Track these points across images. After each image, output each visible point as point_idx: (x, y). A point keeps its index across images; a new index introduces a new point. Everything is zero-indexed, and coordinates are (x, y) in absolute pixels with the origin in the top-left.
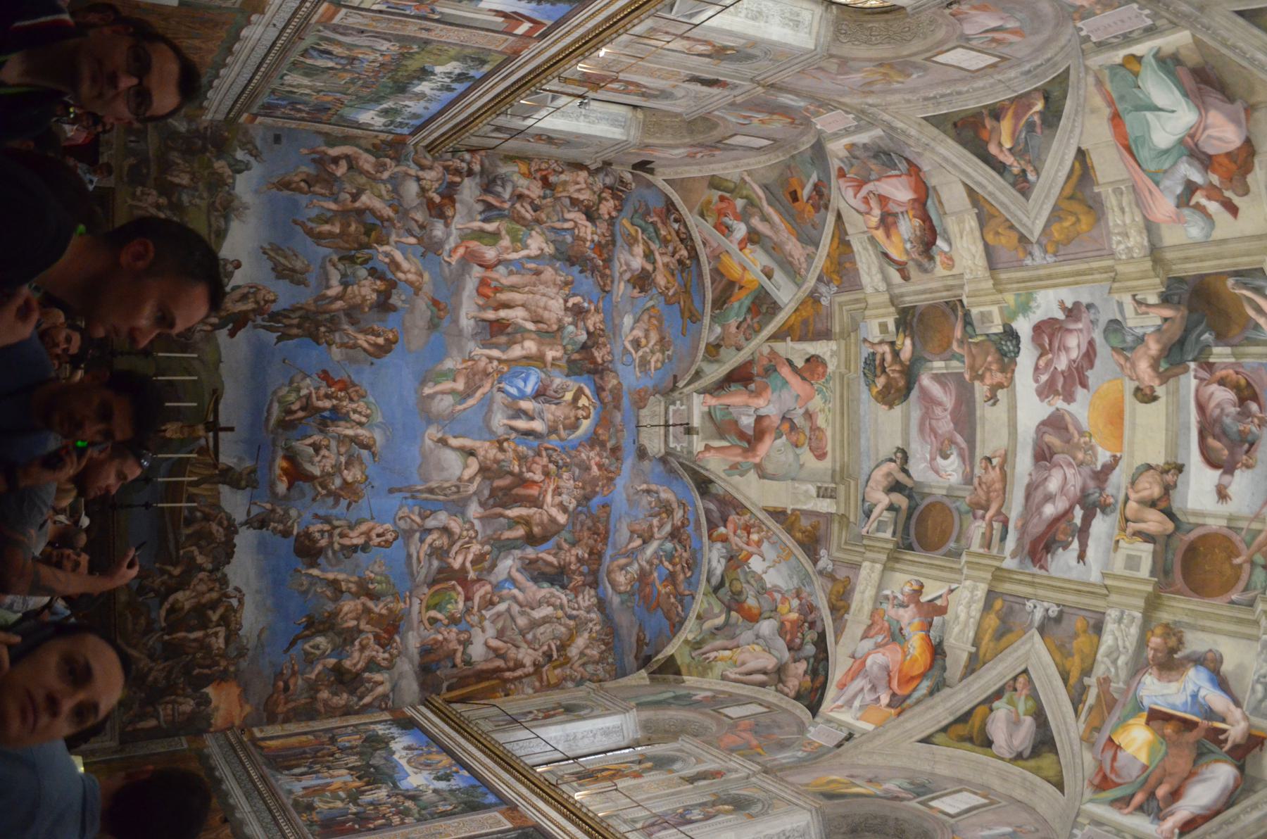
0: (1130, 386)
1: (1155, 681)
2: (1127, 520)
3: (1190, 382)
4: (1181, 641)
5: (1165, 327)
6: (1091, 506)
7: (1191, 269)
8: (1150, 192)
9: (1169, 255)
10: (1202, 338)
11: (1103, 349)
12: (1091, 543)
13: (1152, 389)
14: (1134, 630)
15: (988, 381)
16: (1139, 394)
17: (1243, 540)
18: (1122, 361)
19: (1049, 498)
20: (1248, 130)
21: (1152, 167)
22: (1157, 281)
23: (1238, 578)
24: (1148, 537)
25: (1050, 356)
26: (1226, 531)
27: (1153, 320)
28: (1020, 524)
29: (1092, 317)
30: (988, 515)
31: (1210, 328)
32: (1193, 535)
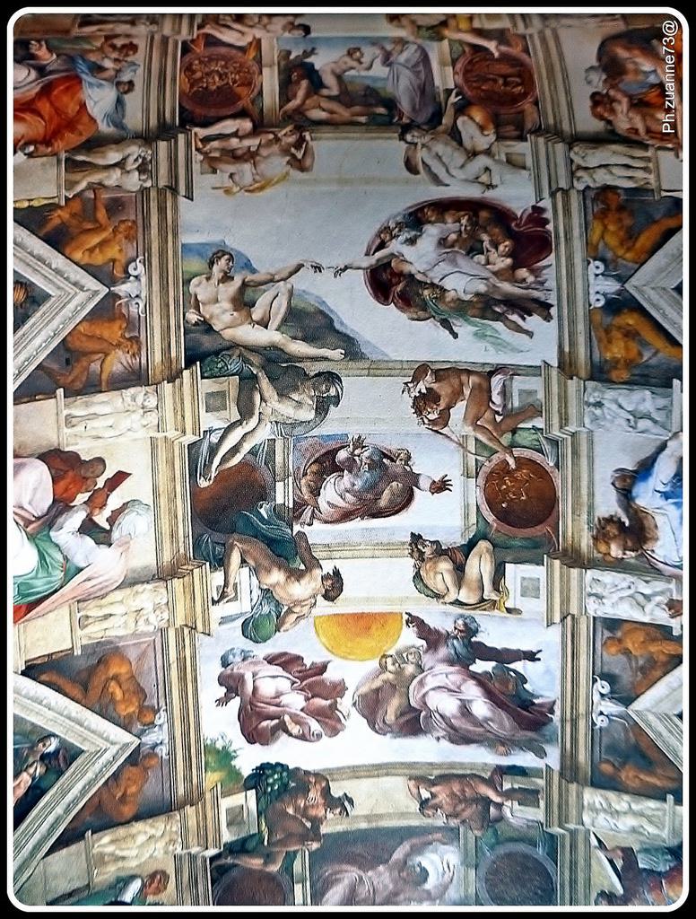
0: (324, 607)
2: (482, 600)
3: (317, 533)
5: (252, 563)
6: (469, 649)
10: (266, 517)
11: (277, 645)
12: (513, 646)
15: (321, 812)
19: (465, 710)
24: (499, 573)
25: (287, 718)
26: (481, 481)
27: (241, 576)
28: (502, 749)
29: (238, 659)
30: (498, 799)
32: (490, 518)
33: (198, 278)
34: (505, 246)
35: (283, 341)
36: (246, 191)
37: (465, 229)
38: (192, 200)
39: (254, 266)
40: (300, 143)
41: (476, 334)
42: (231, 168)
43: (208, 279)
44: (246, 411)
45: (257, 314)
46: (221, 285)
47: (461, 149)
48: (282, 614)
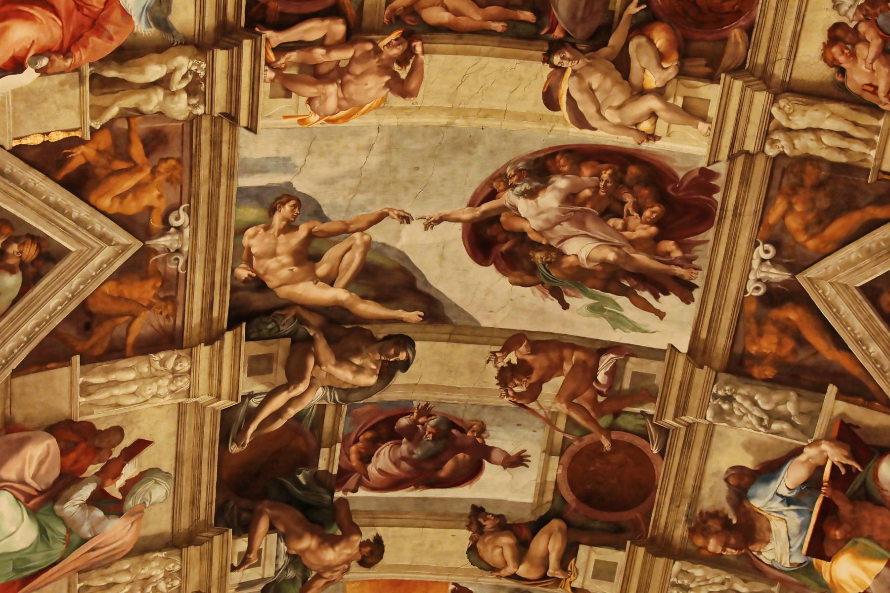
0: (357, 573)
1: (769, 547)
2: (545, 577)
4: (715, 515)
7: (208, 496)
8: (93, 550)
9: (185, 523)
10: (304, 482)
13: (363, 545)
14: (698, 572)
16: (369, 560)
17: (580, 438)
18: (322, 582)
20: (37, 428)
21: (59, 548)
22: (217, 539)
23: (631, 445)
24: (569, 554)
26: (566, 458)
31: (292, 473)
32: (569, 497)
33: (254, 227)
34: (652, 211)
35: (351, 300)
36: (328, 121)
37: (605, 186)
38: (255, 132)
39: (325, 213)
40: (410, 53)
41: (591, 308)
42: (311, 91)
43: (267, 229)
44: (295, 375)
45: (322, 269)
46: (282, 236)
47: (626, 82)
48: (309, 579)
